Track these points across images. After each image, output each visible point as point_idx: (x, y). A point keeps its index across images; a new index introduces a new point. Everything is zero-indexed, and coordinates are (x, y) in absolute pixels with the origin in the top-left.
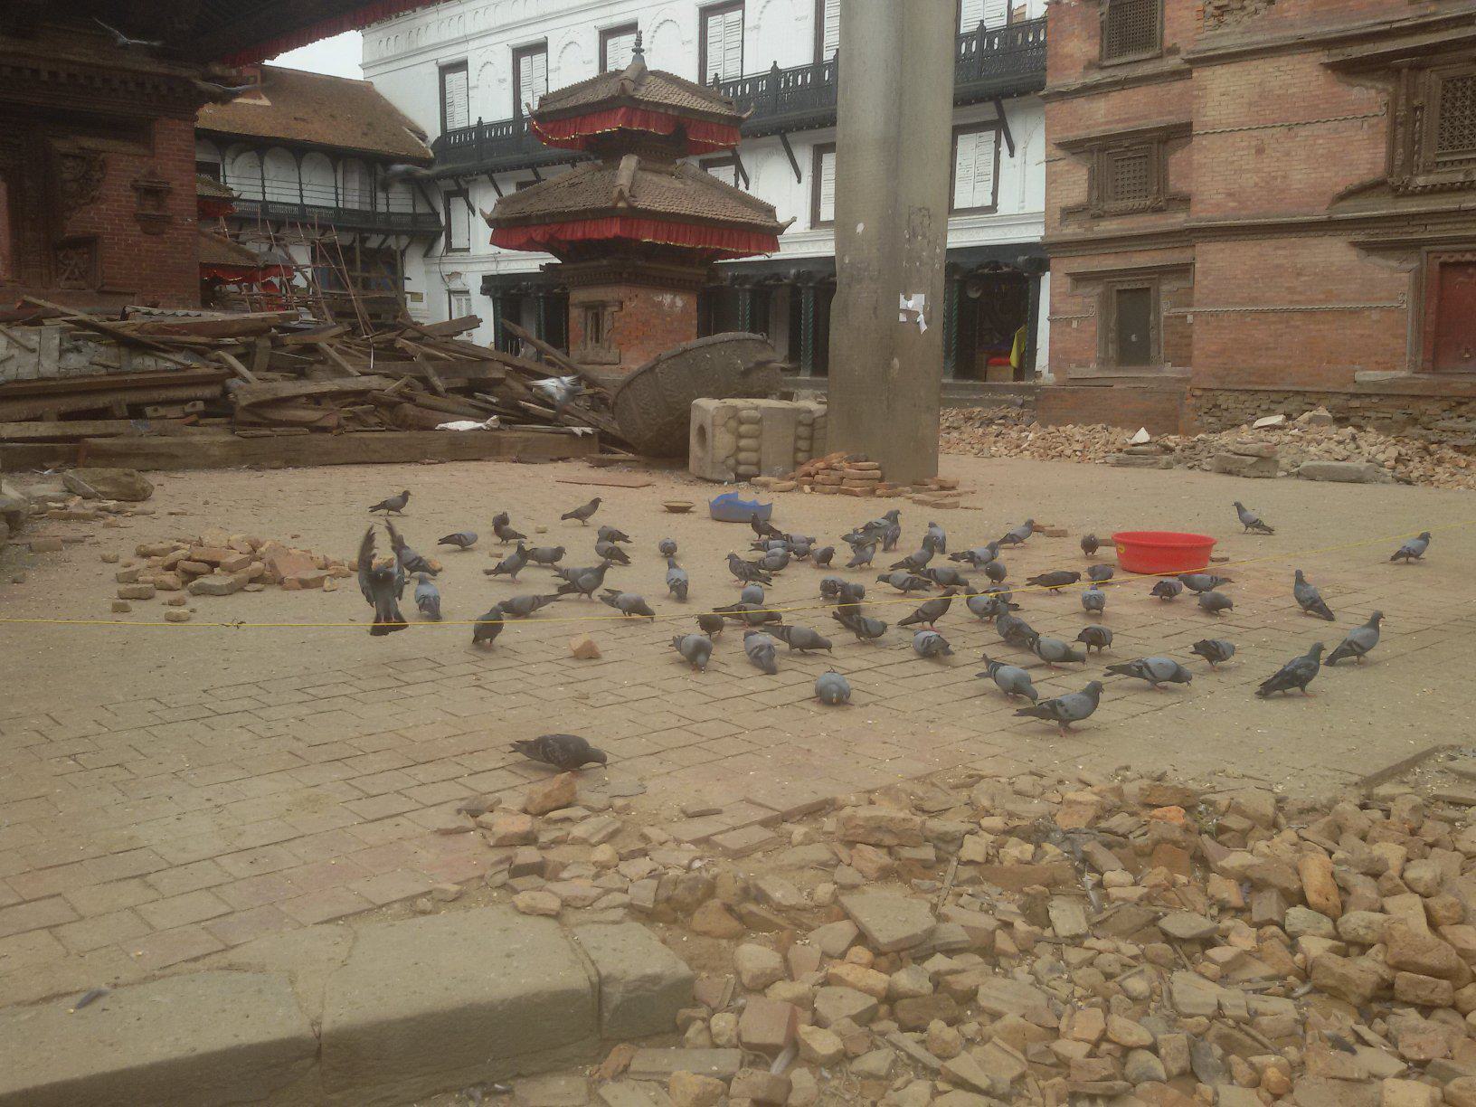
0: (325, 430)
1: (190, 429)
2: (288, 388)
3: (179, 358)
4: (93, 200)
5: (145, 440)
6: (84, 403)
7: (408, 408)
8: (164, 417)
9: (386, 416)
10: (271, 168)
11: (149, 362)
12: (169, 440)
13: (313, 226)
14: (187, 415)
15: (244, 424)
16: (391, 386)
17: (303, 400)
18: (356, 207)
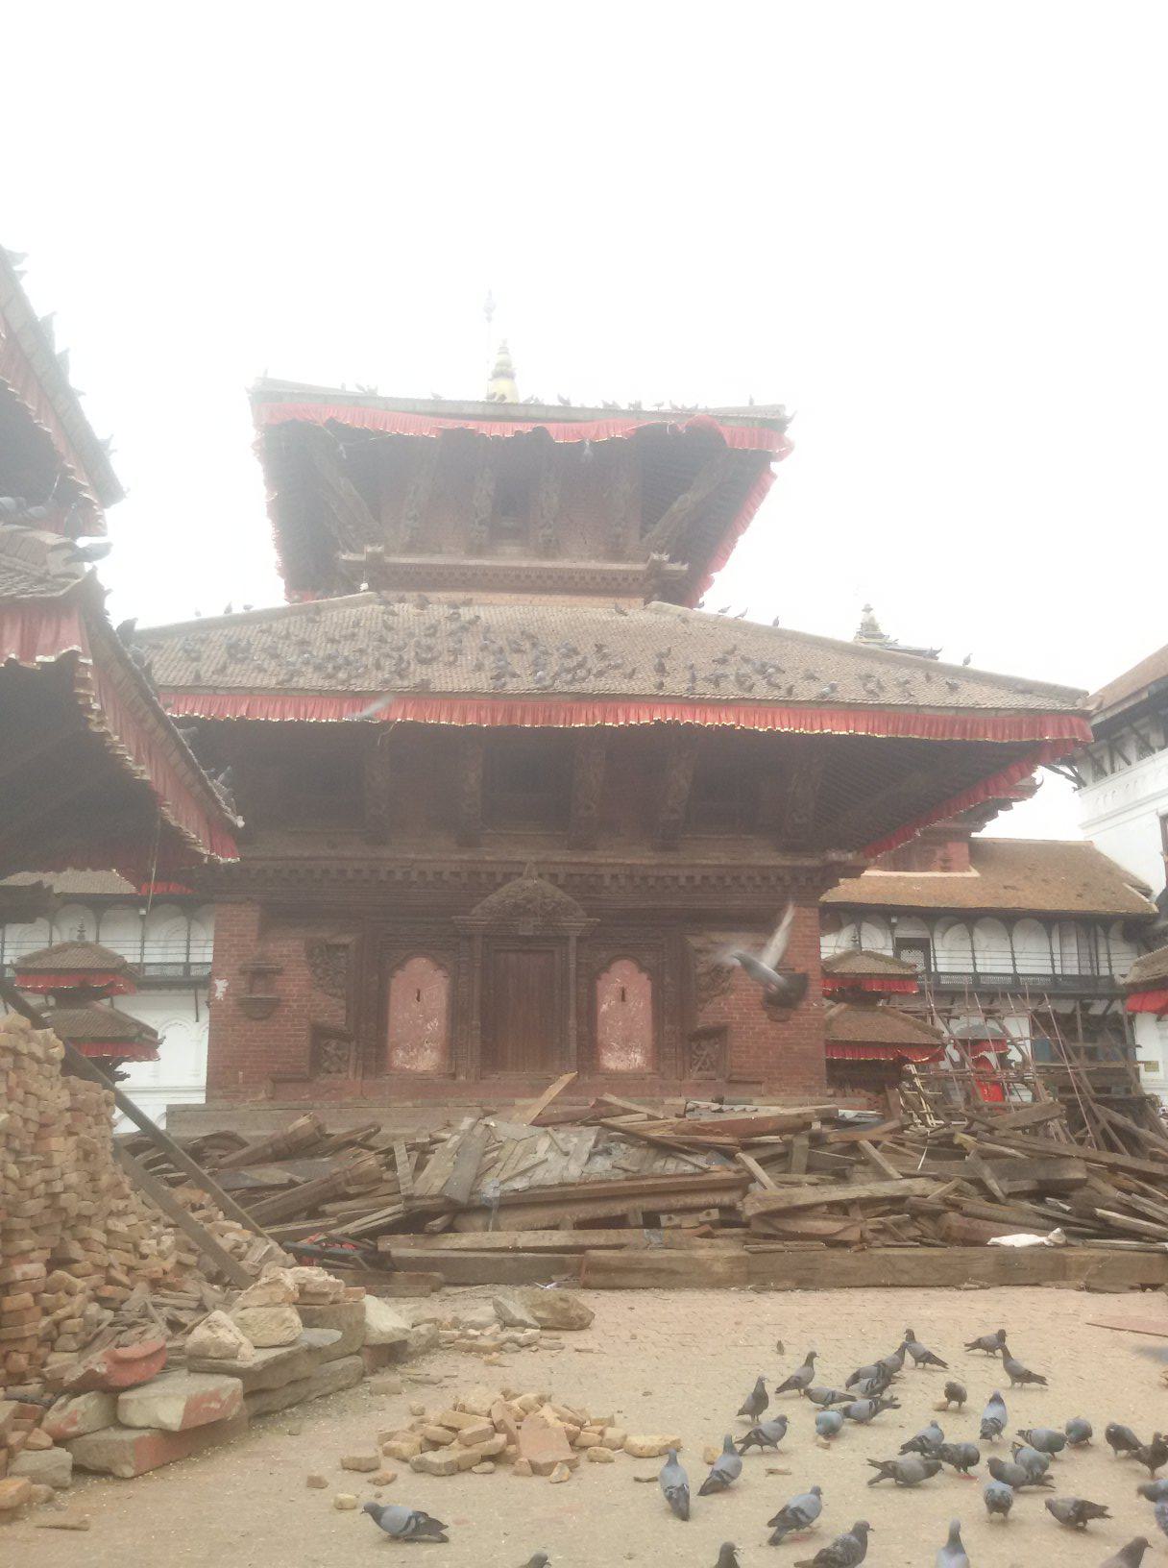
0: (846, 1244)
1: (700, 1241)
2: (806, 1195)
3: (701, 1161)
4: (724, 991)
5: (647, 1254)
6: (601, 1210)
7: (953, 1217)
8: (679, 1227)
9: (928, 1226)
10: (981, 938)
11: (671, 1166)
12: (674, 1253)
13: (1024, 996)
14: (702, 1224)
15: (757, 1236)
16: (936, 1190)
17: (825, 1208)
18: (1076, 972)
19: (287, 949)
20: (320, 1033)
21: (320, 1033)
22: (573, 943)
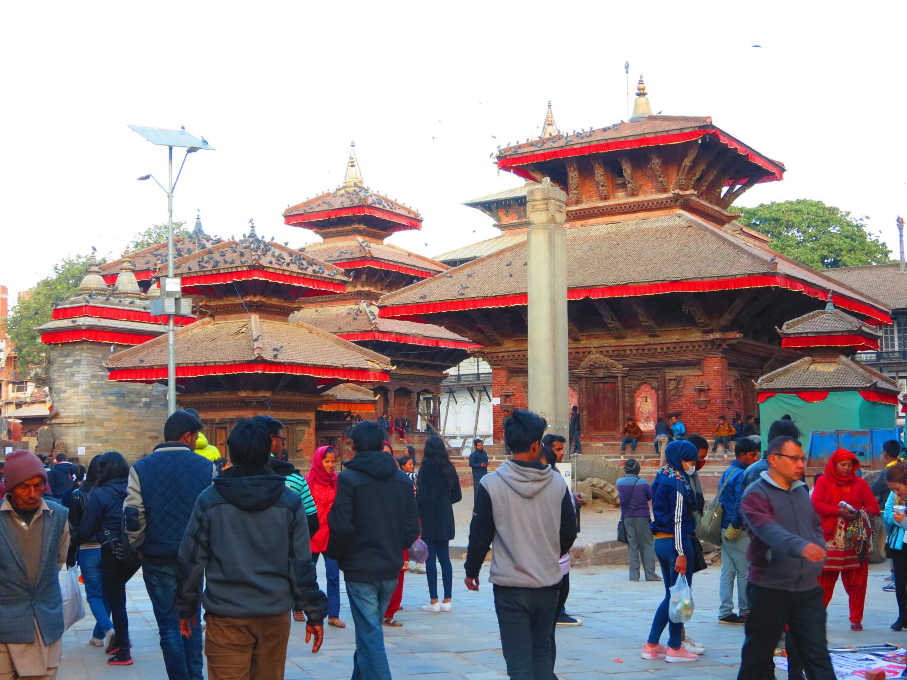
22: (619, 379)
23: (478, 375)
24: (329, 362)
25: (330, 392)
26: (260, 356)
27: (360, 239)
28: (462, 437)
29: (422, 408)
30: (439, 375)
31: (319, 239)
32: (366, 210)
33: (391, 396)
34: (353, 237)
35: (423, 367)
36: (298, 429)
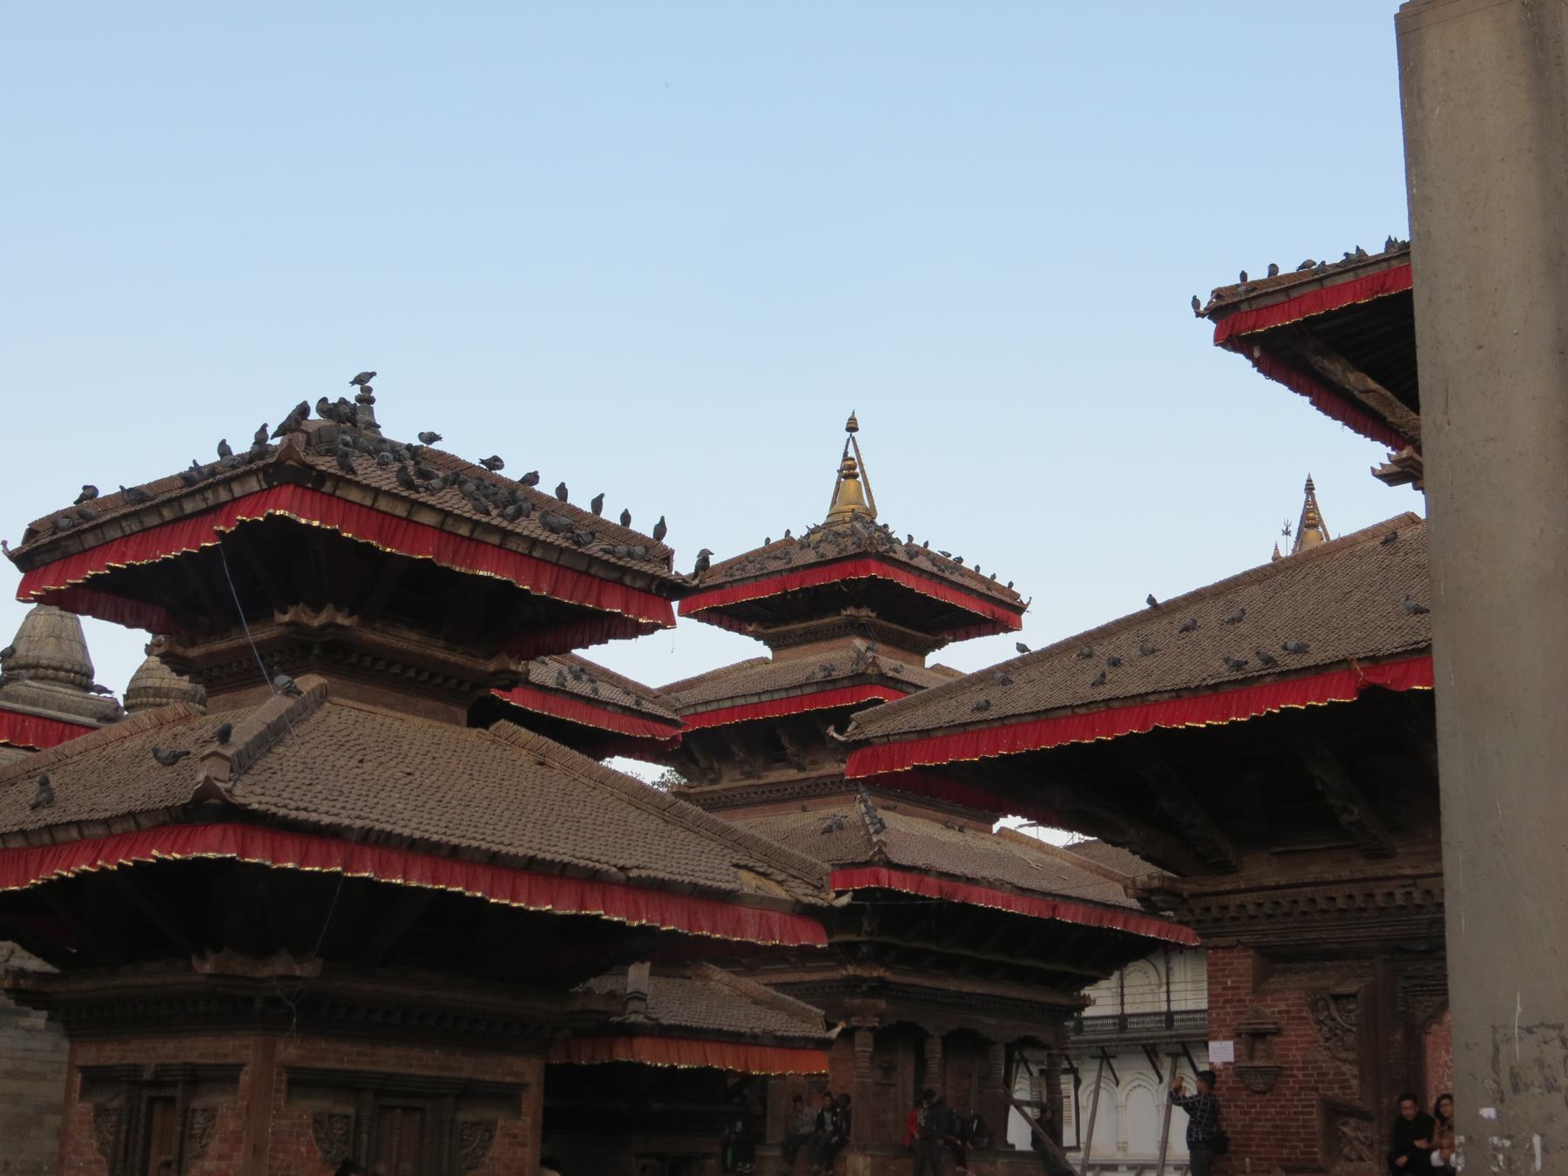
19: (1283, 1001)
20: (1335, 1112)
21: (1335, 1112)
23: (1170, 1015)
24: (560, 851)
25: (600, 985)
26: (208, 789)
27: (859, 643)
28: (1131, 1167)
29: (1022, 1090)
30: (1063, 1000)
31: (760, 650)
32: (873, 564)
33: (934, 1050)
34: (843, 642)
35: (1021, 976)
36: (464, 1116)
